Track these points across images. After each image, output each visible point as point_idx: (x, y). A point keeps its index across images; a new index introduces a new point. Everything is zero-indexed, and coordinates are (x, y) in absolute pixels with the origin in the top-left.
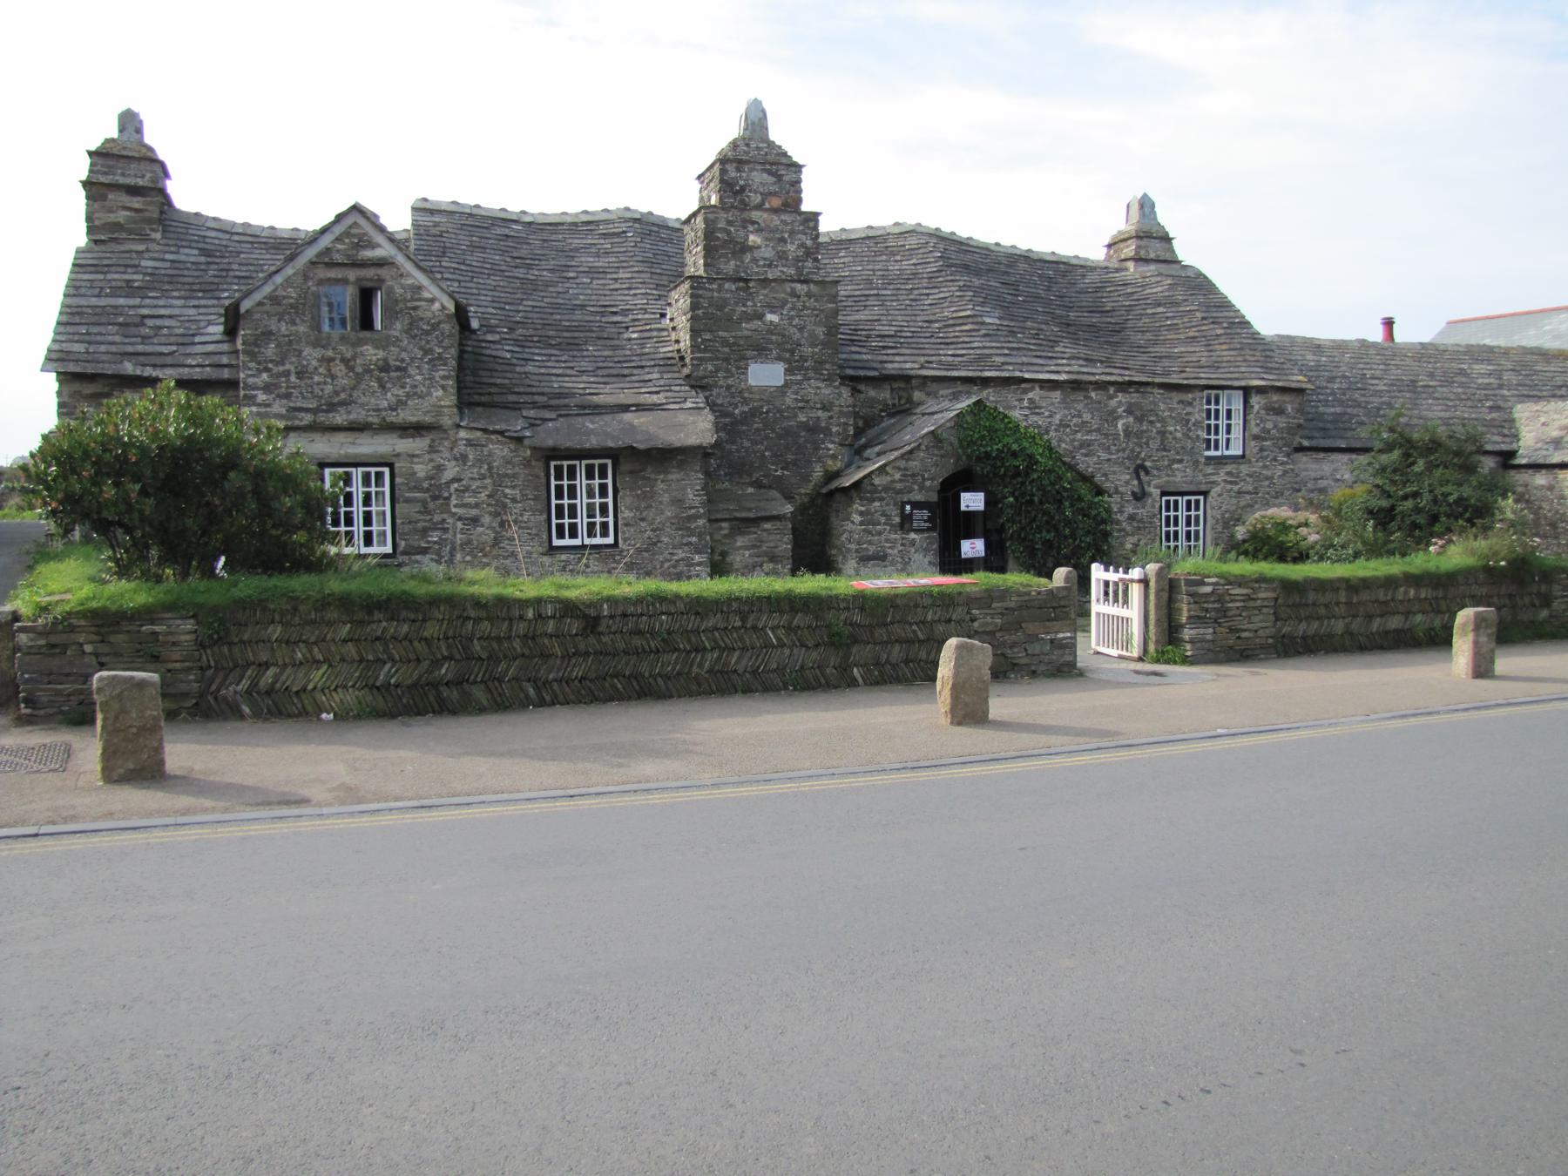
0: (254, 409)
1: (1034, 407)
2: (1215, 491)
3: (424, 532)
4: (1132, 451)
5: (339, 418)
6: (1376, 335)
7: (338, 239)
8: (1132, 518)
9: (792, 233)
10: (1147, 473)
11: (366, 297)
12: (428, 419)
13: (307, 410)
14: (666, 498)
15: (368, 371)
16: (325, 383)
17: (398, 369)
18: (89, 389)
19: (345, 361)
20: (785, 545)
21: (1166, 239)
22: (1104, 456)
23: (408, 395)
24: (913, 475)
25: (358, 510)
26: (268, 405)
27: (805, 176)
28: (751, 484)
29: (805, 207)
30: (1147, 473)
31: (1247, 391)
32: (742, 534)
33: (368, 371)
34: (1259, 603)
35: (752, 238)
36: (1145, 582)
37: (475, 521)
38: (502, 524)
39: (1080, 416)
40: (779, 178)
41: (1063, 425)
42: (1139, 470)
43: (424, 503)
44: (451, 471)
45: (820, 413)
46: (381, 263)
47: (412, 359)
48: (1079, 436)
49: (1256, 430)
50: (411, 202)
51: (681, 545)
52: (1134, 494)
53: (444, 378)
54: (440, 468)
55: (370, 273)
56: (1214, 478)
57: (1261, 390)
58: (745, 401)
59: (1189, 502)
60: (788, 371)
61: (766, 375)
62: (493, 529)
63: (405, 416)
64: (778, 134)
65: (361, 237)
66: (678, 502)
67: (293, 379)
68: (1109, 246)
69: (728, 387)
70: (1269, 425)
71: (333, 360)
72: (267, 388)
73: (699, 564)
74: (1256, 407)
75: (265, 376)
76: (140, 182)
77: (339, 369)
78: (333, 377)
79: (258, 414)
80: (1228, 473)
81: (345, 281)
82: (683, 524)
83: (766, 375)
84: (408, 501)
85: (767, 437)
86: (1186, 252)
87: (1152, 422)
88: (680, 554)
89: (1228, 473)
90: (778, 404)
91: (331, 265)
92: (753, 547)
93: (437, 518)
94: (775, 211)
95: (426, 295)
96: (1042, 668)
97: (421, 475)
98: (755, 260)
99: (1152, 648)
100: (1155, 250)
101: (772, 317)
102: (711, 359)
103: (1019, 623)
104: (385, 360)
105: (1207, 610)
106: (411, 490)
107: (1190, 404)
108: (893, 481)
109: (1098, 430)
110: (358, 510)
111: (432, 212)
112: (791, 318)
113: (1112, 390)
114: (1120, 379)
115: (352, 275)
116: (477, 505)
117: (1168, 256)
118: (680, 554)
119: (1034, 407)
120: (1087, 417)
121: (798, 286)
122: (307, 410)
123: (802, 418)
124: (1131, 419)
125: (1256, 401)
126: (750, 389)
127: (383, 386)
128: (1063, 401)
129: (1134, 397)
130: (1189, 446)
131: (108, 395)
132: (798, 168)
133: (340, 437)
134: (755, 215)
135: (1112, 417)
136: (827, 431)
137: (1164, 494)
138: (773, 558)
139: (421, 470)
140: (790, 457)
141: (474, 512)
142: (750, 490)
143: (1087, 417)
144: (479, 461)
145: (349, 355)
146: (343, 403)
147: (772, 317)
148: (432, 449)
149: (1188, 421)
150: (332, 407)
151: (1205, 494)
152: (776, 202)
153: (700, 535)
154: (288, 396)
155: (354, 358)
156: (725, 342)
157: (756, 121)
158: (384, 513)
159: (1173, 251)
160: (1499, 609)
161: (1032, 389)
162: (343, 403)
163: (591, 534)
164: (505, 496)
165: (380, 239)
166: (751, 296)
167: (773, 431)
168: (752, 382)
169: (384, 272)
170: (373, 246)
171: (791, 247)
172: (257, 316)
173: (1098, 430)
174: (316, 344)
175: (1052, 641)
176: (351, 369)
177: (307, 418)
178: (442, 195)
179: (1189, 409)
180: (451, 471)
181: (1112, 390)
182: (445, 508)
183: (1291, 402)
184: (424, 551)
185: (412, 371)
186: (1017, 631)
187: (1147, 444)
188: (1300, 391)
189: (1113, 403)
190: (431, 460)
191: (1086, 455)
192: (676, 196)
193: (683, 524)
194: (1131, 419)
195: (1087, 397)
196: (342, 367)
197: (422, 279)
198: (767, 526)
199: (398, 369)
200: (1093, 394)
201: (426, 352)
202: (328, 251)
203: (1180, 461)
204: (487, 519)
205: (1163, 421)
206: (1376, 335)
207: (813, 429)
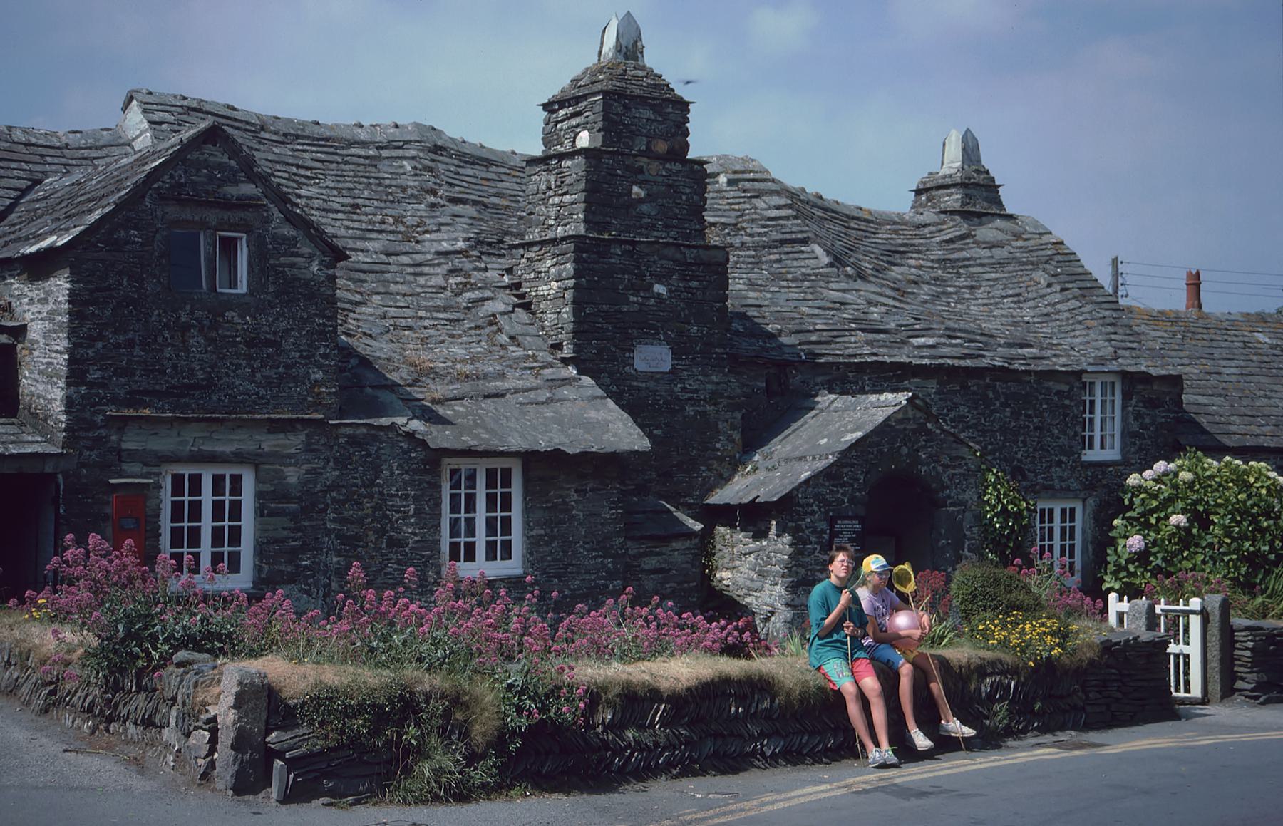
6: (1177, 301)
17: (269, 343)
23: (281, 377)
25: (207, 524)
26: (104, 386)
29: (690, 155)
35: (635, 189)
36: (1204, 614)
53: (325, 356)
60: (676, 355)
61: (653, 358)
67: (137, 351)
68: (918, 192)
71: (186, 328)
87: (1030, 416)
95: (306, 250)
98: (641, 216)
99: (1215, 688)
101: (659, 289)
109: (975, 427)
110: (207, 524)
120: (963, 410)
126: (638, 376)
132: (683, 106)
139: (292, 476)
143: (963, 410)
147: (659, 289)
152: (661, 147)
163: (491, 556)
173: (975, 427)
185: (286, 345)
192: (511, 125)
206: (1177, 301)
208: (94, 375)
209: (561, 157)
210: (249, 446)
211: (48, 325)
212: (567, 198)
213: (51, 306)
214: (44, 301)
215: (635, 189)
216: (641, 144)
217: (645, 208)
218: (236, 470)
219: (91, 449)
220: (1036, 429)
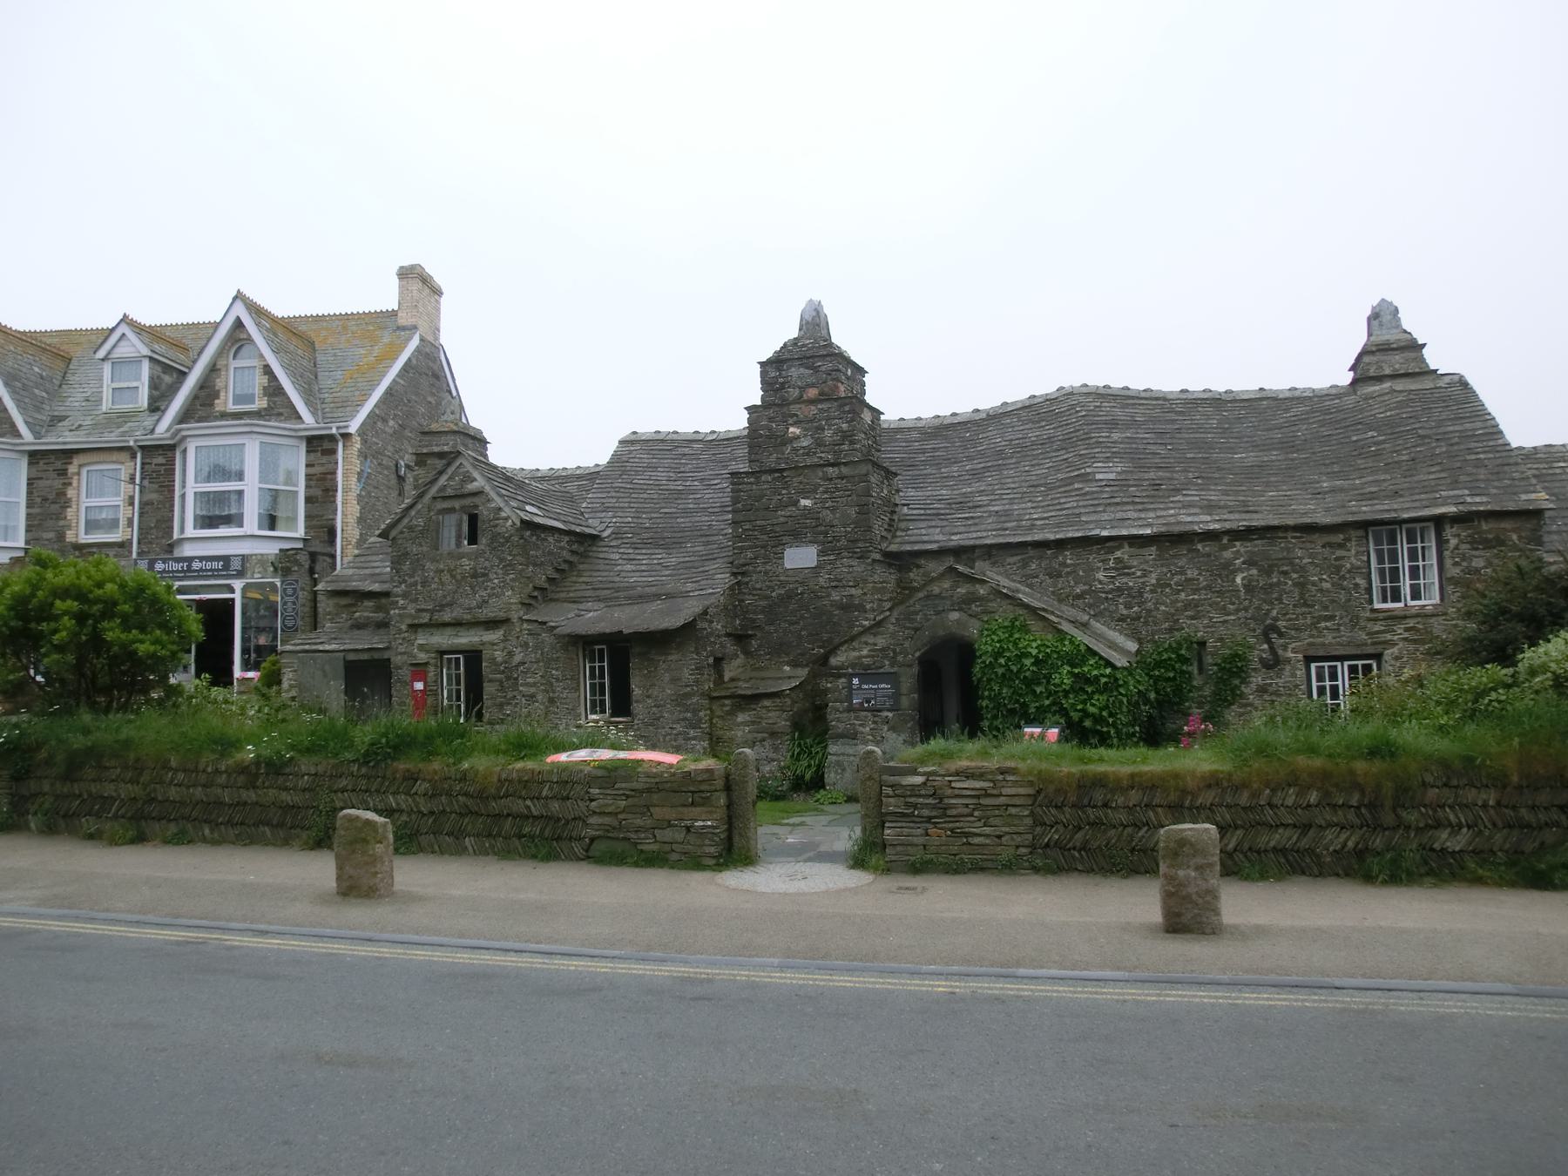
1: (1122, 568)
2: (1388, 654)
3: (501, 705)
4: (1259, 608)
5: (447, 617)
7: (450, 478)
8: (1262, 690)
9: (828, 419)
10: (1281, 635)
11: (473, 520)
12: (502, 615)
14: (667, 677)
15: (464, 578)
17: (484, 575)
18: (344, 601)
19: (450, 571)
20: (783, 723)
21: (1415, 347)
22: (1217, 617)
24: (883, 650)
28: (788, 664)
30: (1281, 635)
31: (1439, 521)
32: (742, 710)
34: (1002, 800)
38: (552, 701)
39: (1182, 573)
40: (816, 370)
41: (1162, 585)
42: (1269, 632)
43: (501, 682)
45: (853, 591)
46: (478, 493)
48: (1183, 595)
49: (1454, 572)
51: (678, 721)
52: (1261, 660)
55: (467, 502)
56: (1389, 636)
57: (1456, 519)
58: (782, 584)
59: (1353, 669)
60: (821, 553)
61: (800, 557)
63: (487, 613)
66: (674, 680)
69: (766, 573)
70: (1478, 563)
72: (405, 595)
73: (694, 738)
74: (1453, 542)
76: (446, 449)
77: (446, 577)
78: (443, 584)
80: (1407, 630)
81: (452, 510)
82: (680, 700)
83: (800, 557)
85: (802, 617)
86: (1436, 358)
87: (1285, 573)
88: (679, 728)
89: (1407, 630)
90: (811, 584)
91: (445, 498)
92: (753, 723)
93: (510, 695)
94: (812, 402)
95: (503, 514)
96: (674, 857)
97: (499, 659)
98: (794, 449)
100: (1397, 362)
101: (805, 502)
102: (751, 547)
103: (648, 808)
104: (474, 568)
105: (915, 806)
107: (1341, 546)
108: (860, 657)
109: (1208, 588)
111: (632, 442)
112: (824, 501)
113: (1225, 541)
114: (1234, 526)
115: (457, 504)
116: (534, 685)
117: (1413, 368)
118: (679, 728)
119: (1122, 568)
121: (831, 469)
123: (835, 596)
124: (1254, 572)
125: (1449, 532)
128: (1160, 557)
129: (1258, 545)
130: (1343, 597)
133: (449, 631)
134: (794, 409)
135: (1228, 570)
136: (861, 608)
137: (1309, 660)
138: (773, 734)
139: (499, 655)
140: (825, 636)
141: (533, 690)
142: (787, 668)
143: (1190, 574)
144: (536, 647)
146: (448, 605)
147: (805, 502)
148: (505, 640)
149: (1338, 569)
150: (442, 607)
151: (1378, 657)
152: (812, 393)
153: (695, 712)
156: (762, 530)
159: (1423, 360)
160: (1223, 829)
161: (1119, 548)
162: (448, 605)
166: (786, 486)
167: (808, 610)
168: (788, 566)
169: (476, 500)
171: (828, 433)
173: (1208, 588)
174: (434, 560)
175: (688, 829)
176: (453, 577)
178: (648, 425)
179: (1340, 553)
180: (518, 658)
181: (1225, 541)
182: (515, 686)
183: (1514, 530)
185: (492, 576)
186: (643, 814)
187: (1280, 599)
188: (1536, 514)
189: (1227, 554)
191: (1192, 618)
193: (680, 700)
194: (1254, 572)
195: (1190, 551)
197: (499, 502)
198: (767, 703)
199: (484, 575)
200: (1199, 547)
201: (502, 560)
203: (1332, 618)
204: (540, 697)
205: (1303, 569)
207: (847, 607)
210: (476, 639)
215: (791, 429)
216: (795, 393)
220: (1295, 585)
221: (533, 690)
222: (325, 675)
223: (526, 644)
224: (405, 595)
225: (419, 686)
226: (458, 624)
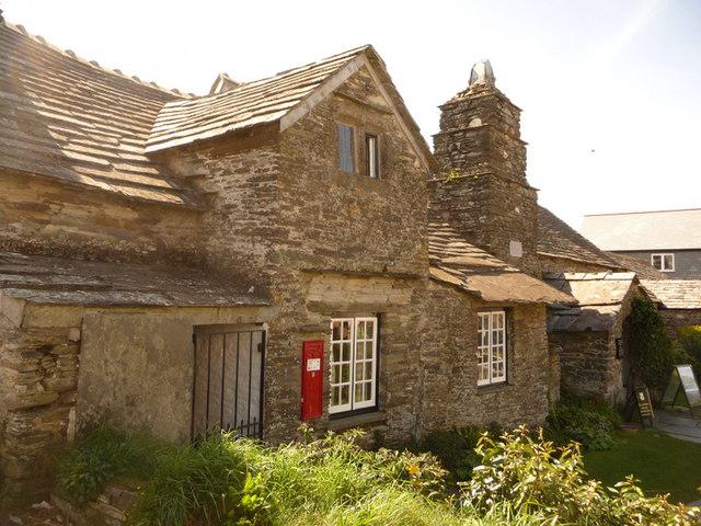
0: (285, 247)
5: (355, 265)
7: (351, 79)
12: (414, 271)
13: (330, 253)
15: (377, 218)
16: (346, 226)
17: (397, 220)
26: (299, 244)
27: (523, 117)
33: (377, 218)
37: (436, 368)
38: (456, 370)
44: (424, 320)
46: (382, 111)
47: (405, 210)
50: (221, 70)
54: (416, 319)
62: (447, 374)
64: (500, 85)
65: (368, 80)
71: (351, 201)
72: (299, 224)
75: (297, 209)
78: (352, 220)
79: (289, 253)
84: (396, 351)
95: (411, 152)
106: (396, 341)
116: (438, 355)
122: (330, 253)
127: (385, 235)
131: (43, 209)
132: (519, 110)
133: (353, 283)
139: (405, 319)
141: (436, 360)
145: (363, 199)
146: (360, 249)
148: (414, 301)
150: (349, 252)
154: (315, 235)
155: (368, 202)
157: (490, 77)
158: (371, 363)
162: (360, 249)
164: (456, 343)
165: (380, 88)
170: (373, 92)
172: (292, 139)
177: (332, 262)
184: (402, 401)
190: (413, 311)
196: (358, 211)
202: (345, 86)
204: (443, 367)
208: (293, 234)
209: (465, 131)
210: (383, 299)
211: (249, 191)
212: (470, 155)
213: (252, 174)
214: (246, 171)
217: (509, 165)
218: (370, 319)
219: (288, 300)
221: (436, 360)
222: (152, 357)
223: (432, 307)
224: (299, 224)
225: (314, 365)
226: (365, 275)
